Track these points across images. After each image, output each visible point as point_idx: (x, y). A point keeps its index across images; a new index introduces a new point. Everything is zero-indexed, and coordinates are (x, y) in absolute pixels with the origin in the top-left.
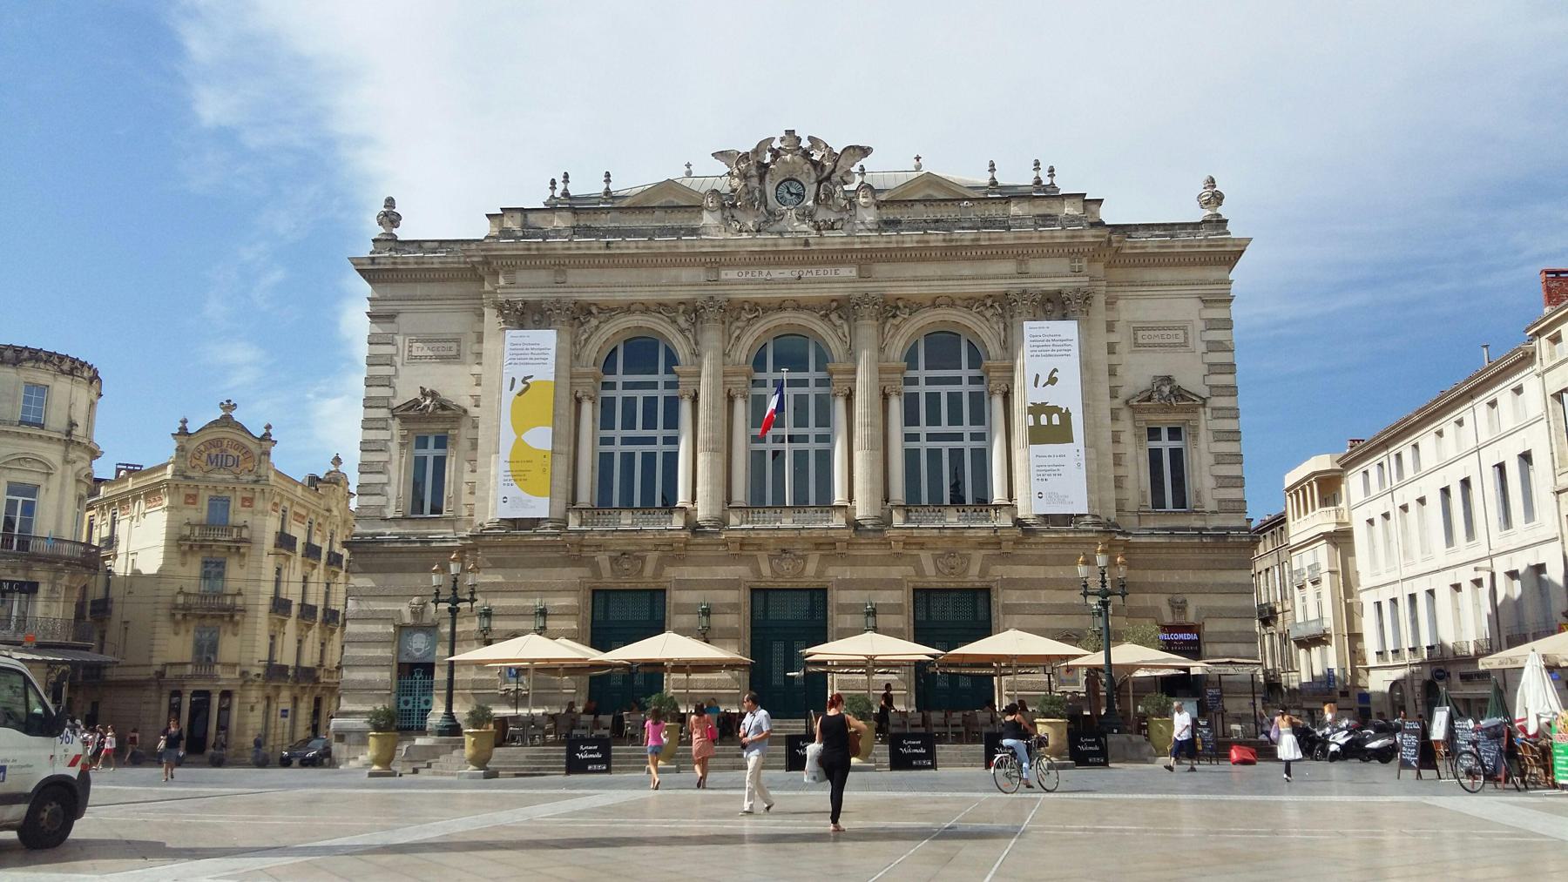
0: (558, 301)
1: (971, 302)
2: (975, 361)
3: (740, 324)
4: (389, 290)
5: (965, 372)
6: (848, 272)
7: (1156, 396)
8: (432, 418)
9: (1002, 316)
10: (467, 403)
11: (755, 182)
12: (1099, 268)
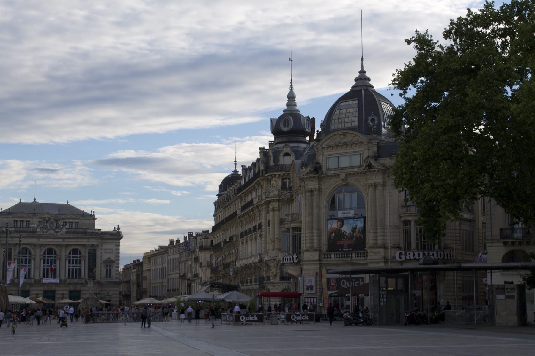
2: (80, 254)
6: (61, 240)
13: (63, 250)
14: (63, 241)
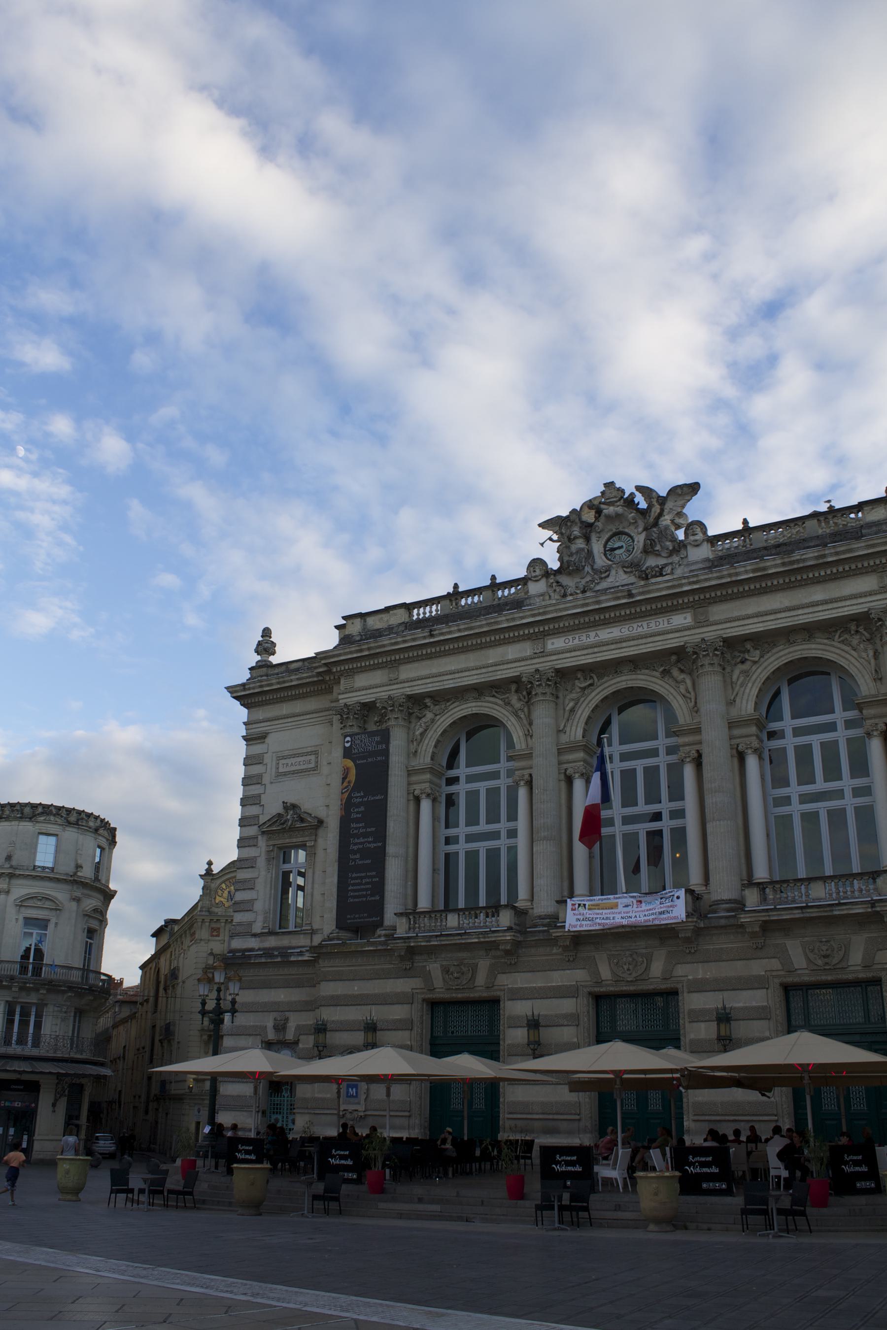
0: (390, 698)
3: (574, 696)
4: (261, 713)
5: (839, 715)
8: (292, 829)
11: (580, 544)
13: (711, 684)
14: (699, 623)
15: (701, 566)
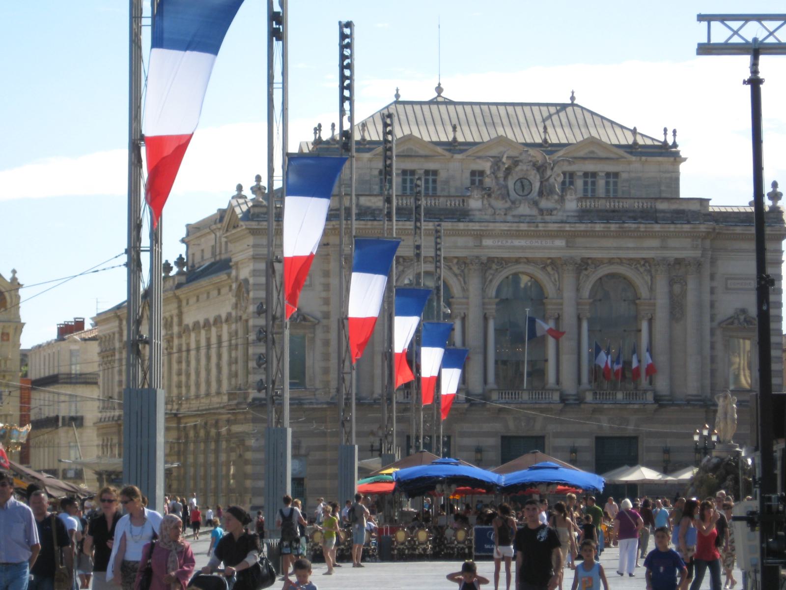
1: (631, 262)
3: (492, 272)
6: (560, 243)
7: (736, 321)
9: (649, 271)
10: (319, 315)
11: (501, 181)
12: (708, 243)
15: (572, 214)
